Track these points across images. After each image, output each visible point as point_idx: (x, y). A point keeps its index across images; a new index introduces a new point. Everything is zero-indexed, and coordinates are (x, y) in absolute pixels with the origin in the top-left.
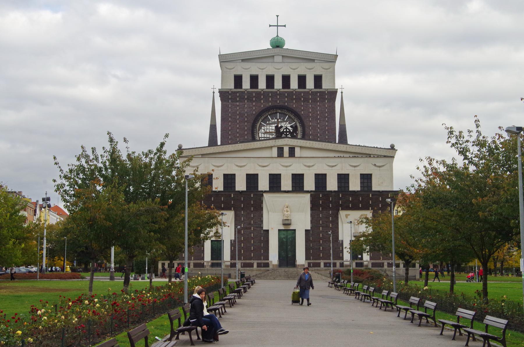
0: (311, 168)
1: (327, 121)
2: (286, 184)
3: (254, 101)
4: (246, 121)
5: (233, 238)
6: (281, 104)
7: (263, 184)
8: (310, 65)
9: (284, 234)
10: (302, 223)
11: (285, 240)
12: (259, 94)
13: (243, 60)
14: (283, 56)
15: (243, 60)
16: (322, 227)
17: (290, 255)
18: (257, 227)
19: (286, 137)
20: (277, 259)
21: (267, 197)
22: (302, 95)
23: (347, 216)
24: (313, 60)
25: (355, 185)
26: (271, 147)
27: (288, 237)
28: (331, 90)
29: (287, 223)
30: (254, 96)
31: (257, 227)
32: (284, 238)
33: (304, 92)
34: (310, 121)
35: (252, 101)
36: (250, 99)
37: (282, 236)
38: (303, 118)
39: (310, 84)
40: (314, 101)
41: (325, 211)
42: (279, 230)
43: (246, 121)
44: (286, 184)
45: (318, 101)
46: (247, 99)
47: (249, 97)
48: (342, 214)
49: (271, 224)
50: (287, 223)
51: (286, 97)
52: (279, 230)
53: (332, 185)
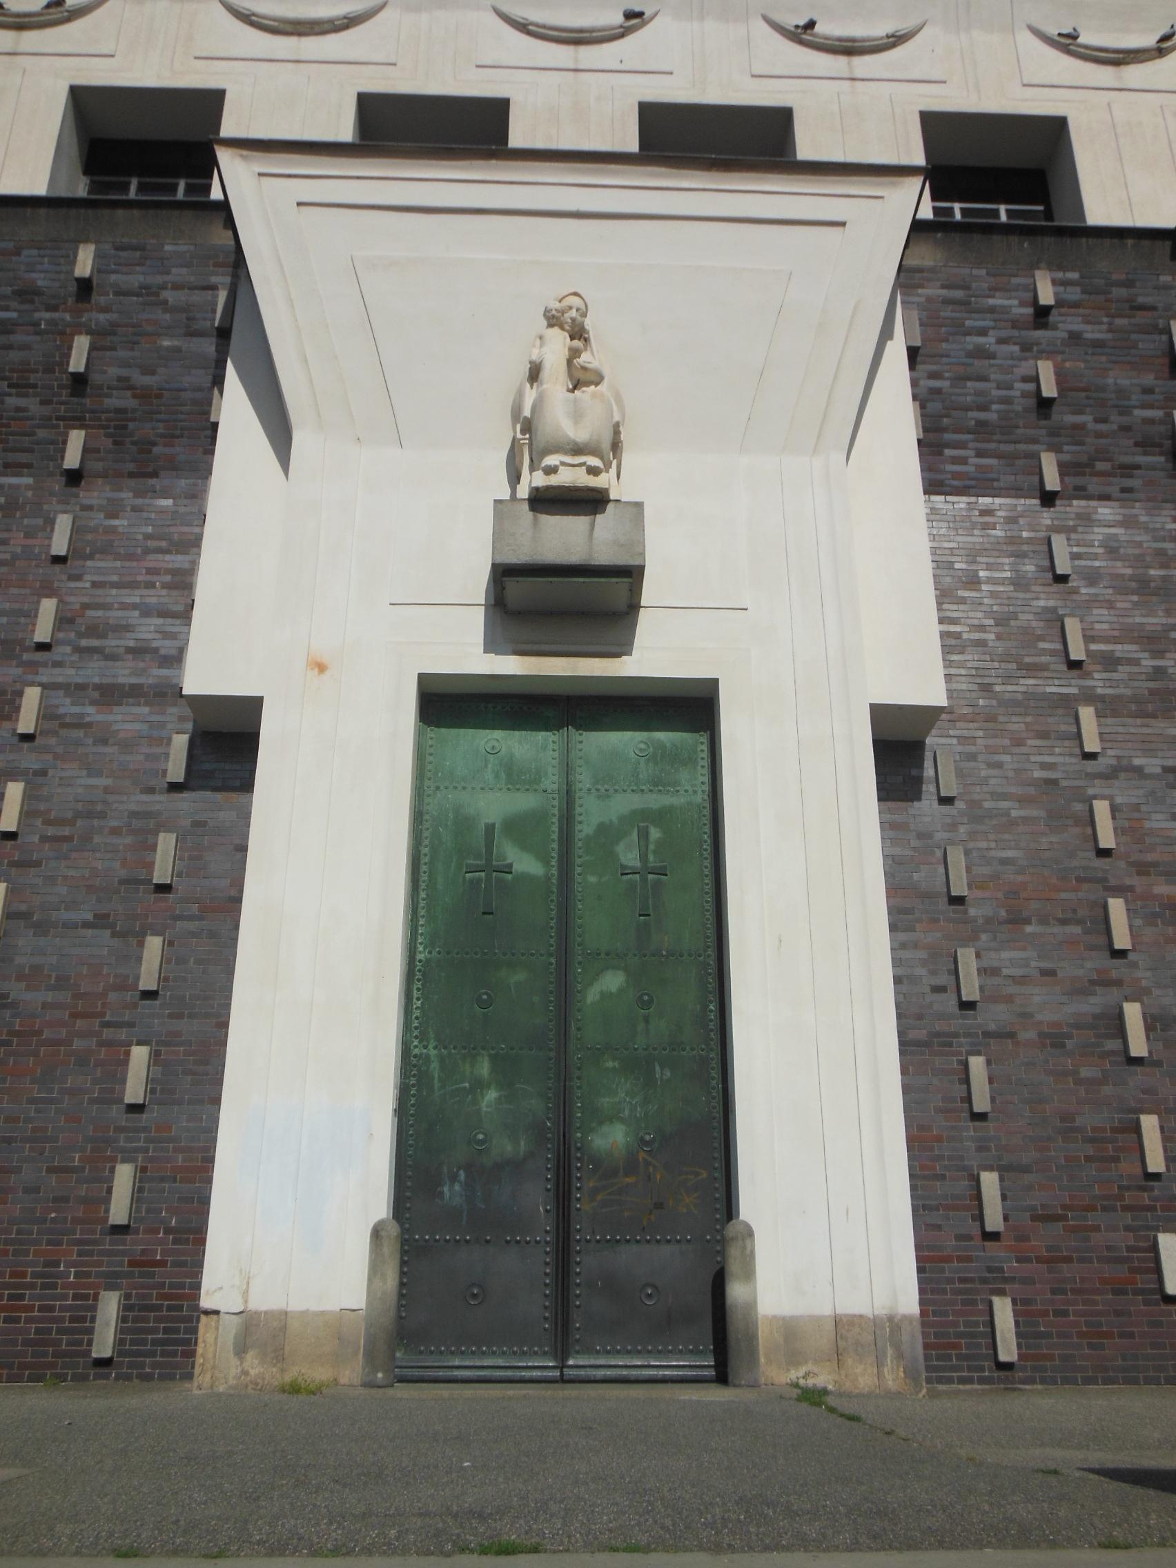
0: (863, 65)
9: (515, 776)
11: (525, 864)
16: (1107, 707)
17: (612, 1138)
18: (110, 695)
20: (381, 1208)
27: (593, 814)
29: (563, 594)
31: (110, 695)
32: (520, 828)
37: (493, 805)
41: (1105, 511)
42: (445, 703)
49: (323, 582)
50: (563, 594)
52: (444, 703)
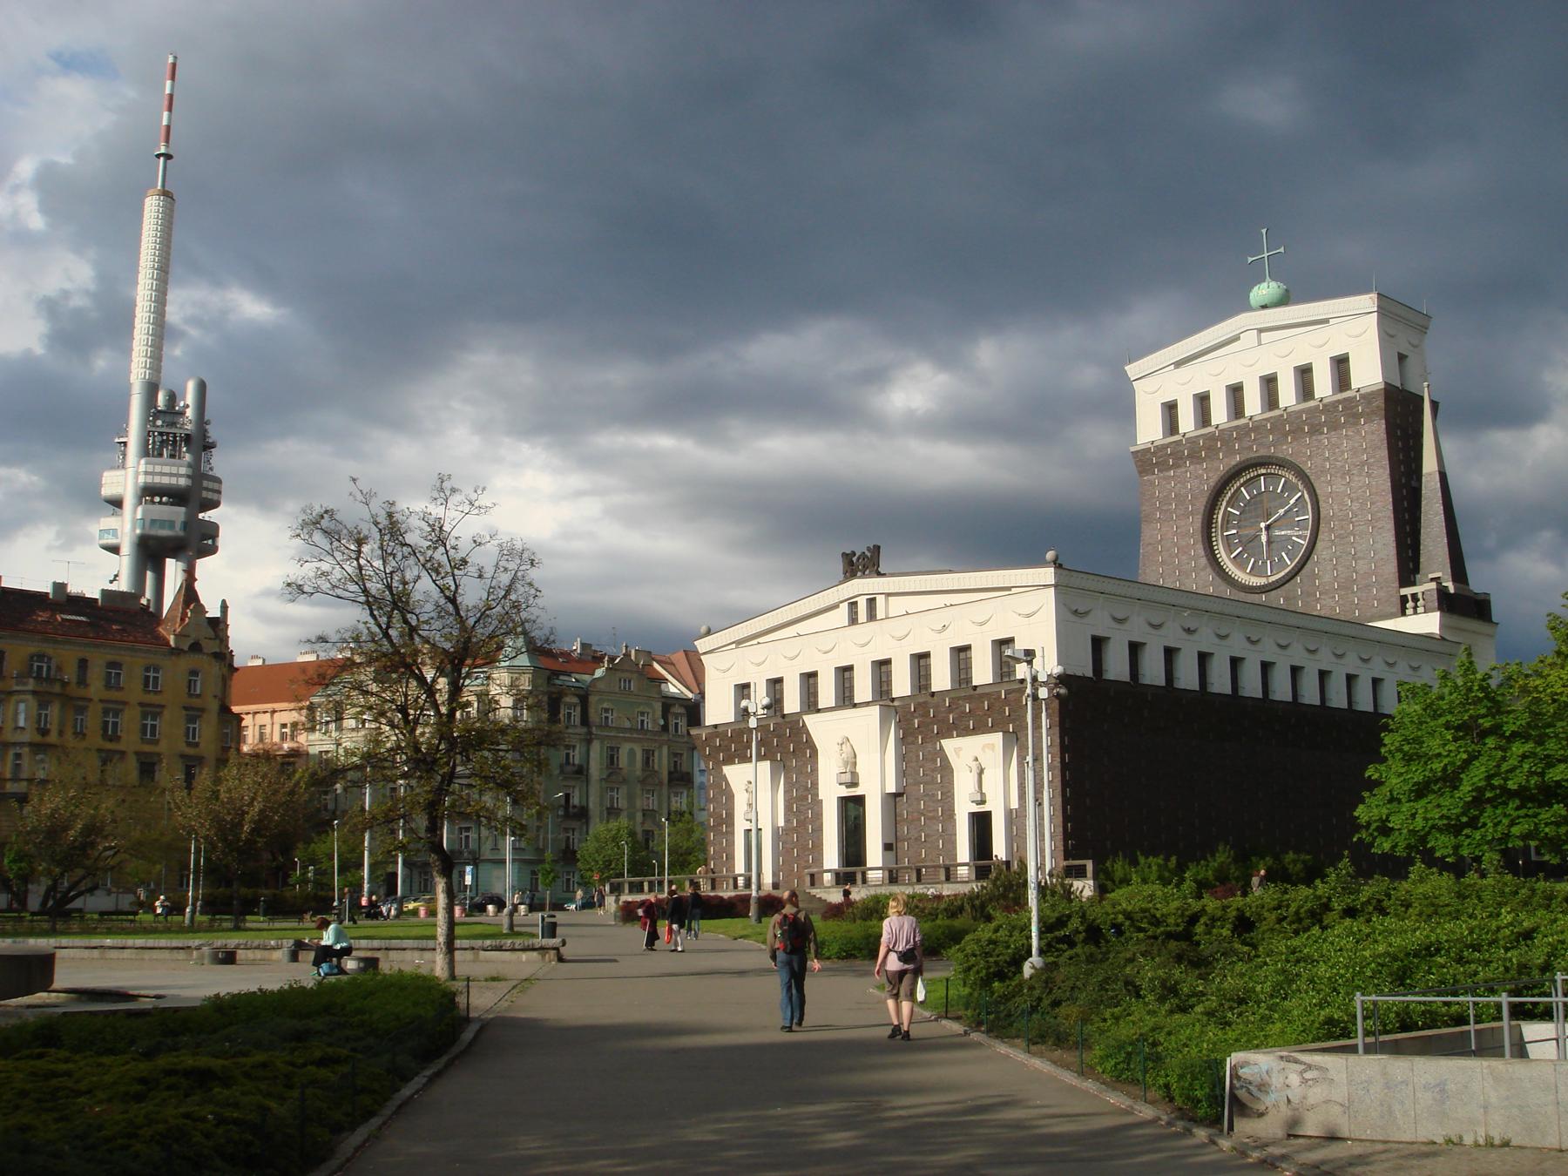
1: (1369, 475)
2: (863, 687)
3: (1204, 460)
4: (1192, 513)
5: (781, 823)
6: (1263, 452)
7: (827, 693)
8: (1319, 333)
10: (878, 777)
12: (1211, 438)
13: (1178, 364)
14: (1260, 331)
15: (1178, 364)
16: (925, 784)
19: (864, 576)
21: (810, 721)
22: (1318, 421)
23: (957, 750)
24: (1326, 321)
25: (983, 672)
26: (835, 606)
28: (1369, 390)
30: (1211, 444)
33: (1308, 411)
34: (1329, 483)
35: (1200, 460)
36: (1194, 457)
38: (1312, 478)
39: (1323, 386)
40: (1335, 427)
43: (1192, 513)
44: (863, 687)
45: (1344, 425)
46: (1190, 456)
47: (1195, 451)
48: (949, 745)
51: (1271, 431)
53: (941, 679)
